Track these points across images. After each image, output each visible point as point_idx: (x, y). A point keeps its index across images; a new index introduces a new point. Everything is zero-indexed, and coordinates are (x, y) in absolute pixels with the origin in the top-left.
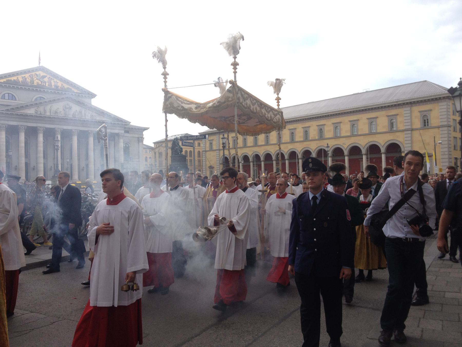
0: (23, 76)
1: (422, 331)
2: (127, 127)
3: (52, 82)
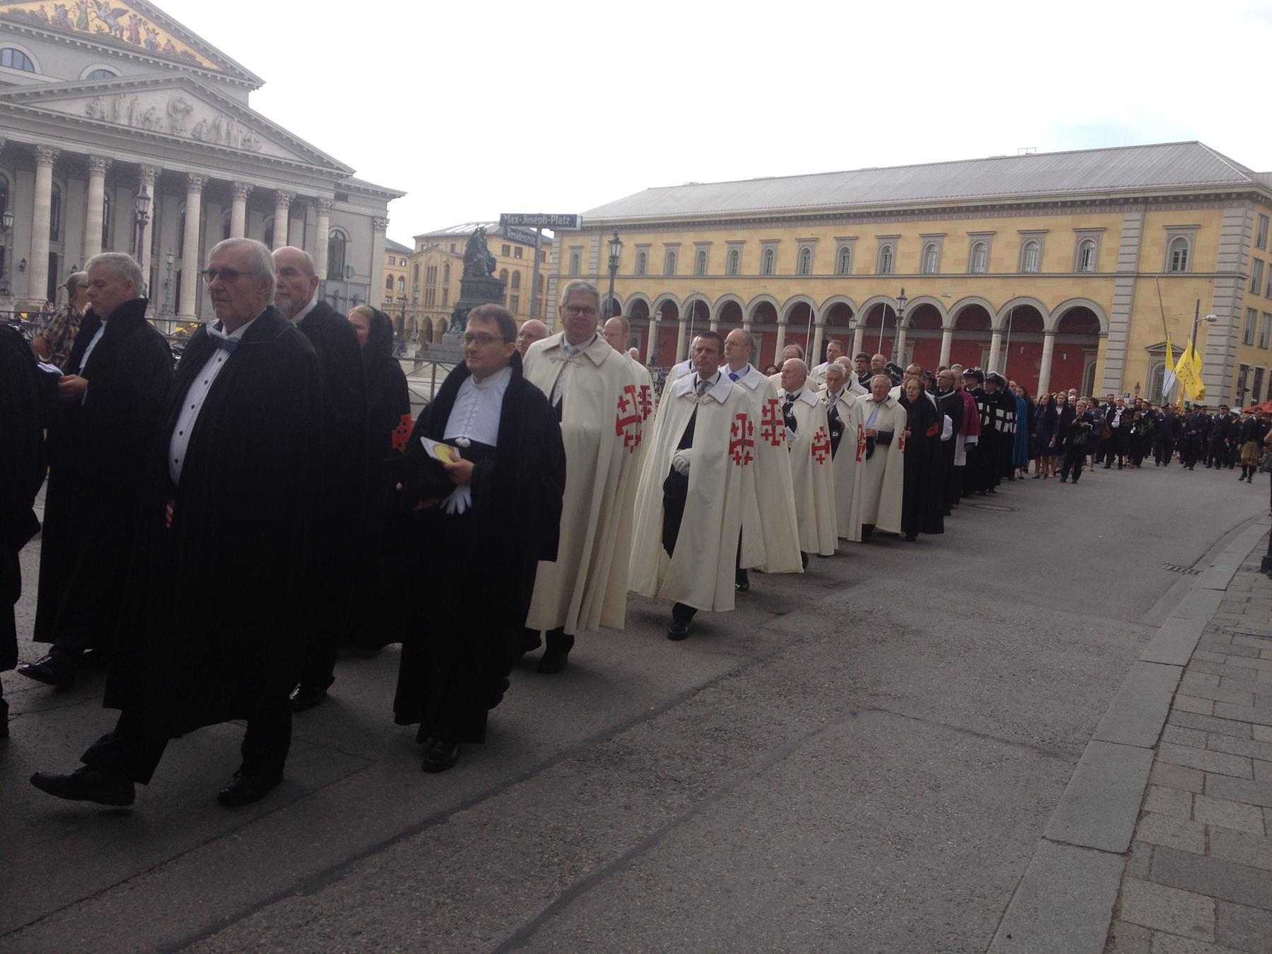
1: (1207, 834)
2: (344, 182)
3: (142, 30)
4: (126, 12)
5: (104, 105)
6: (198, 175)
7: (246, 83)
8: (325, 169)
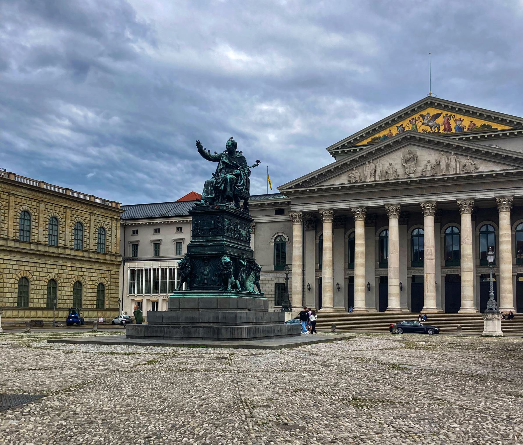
0: (398, 125)
4: (441, 113)
5: (356, 174)
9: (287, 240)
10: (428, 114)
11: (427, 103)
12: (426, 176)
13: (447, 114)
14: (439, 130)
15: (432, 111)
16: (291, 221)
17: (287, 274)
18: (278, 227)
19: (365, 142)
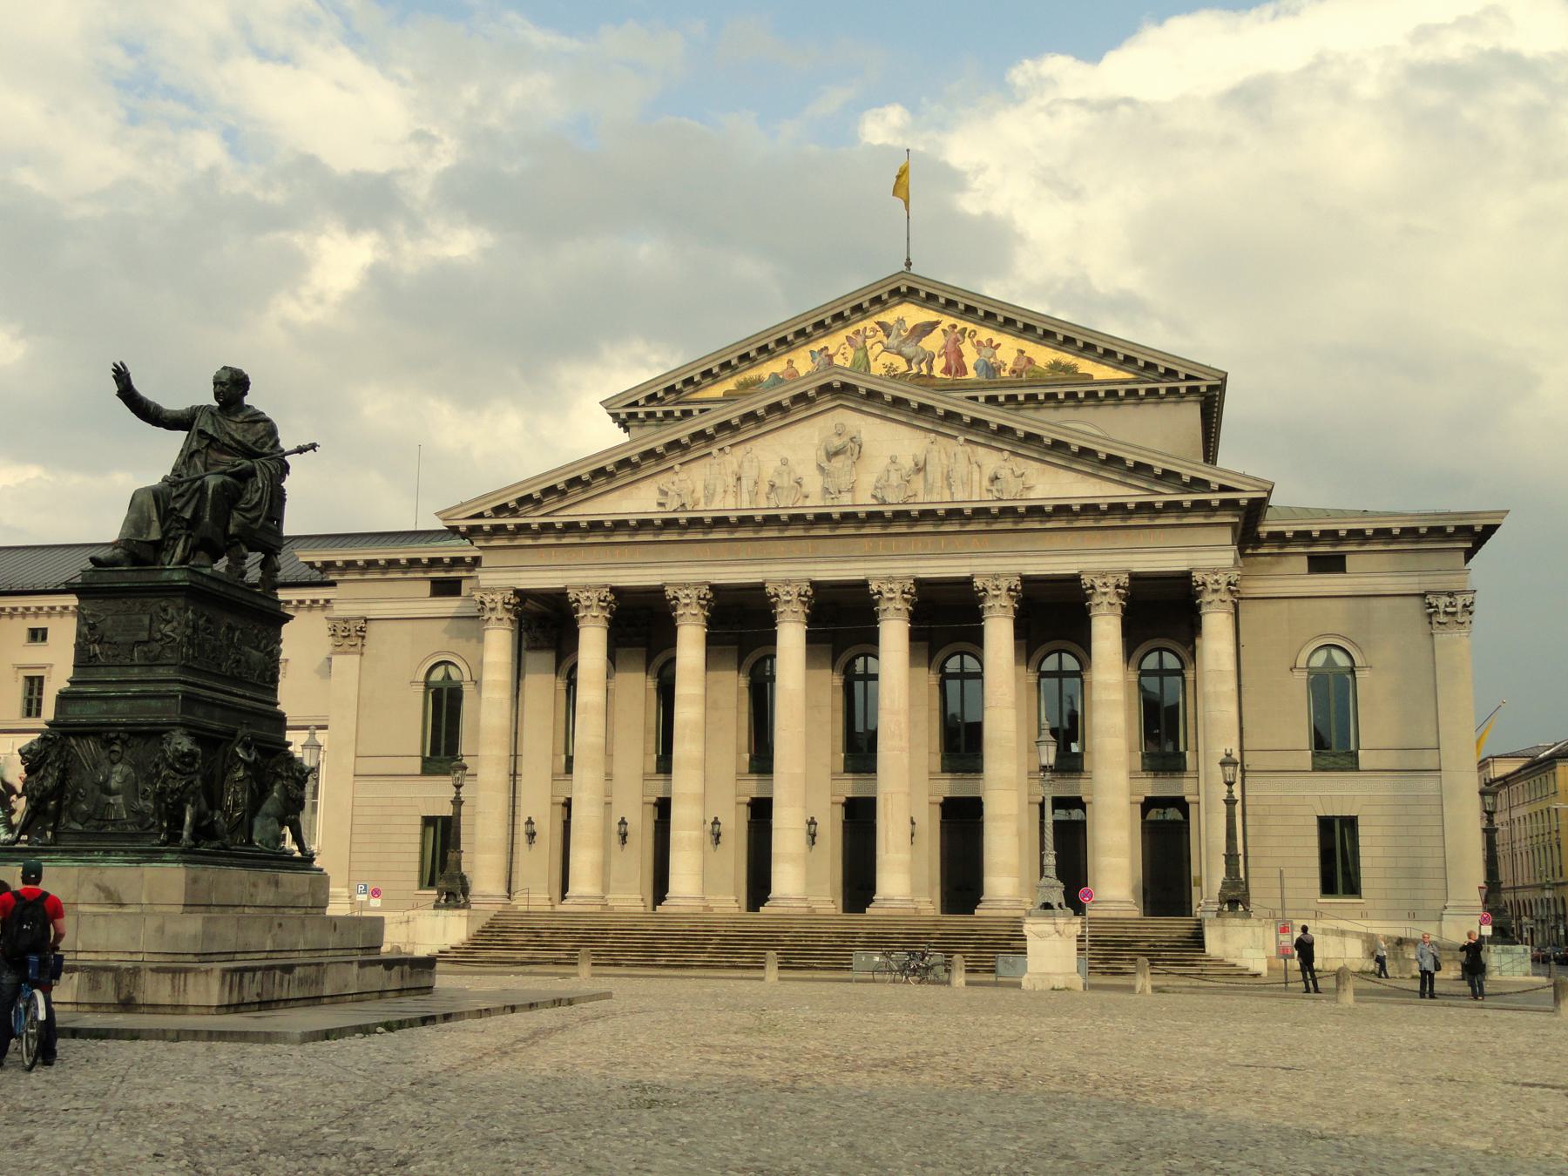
0: (816, 347)
4: (938, 323)
6: (890, 579)
7: (1183, 387)
8: (1187, 499)
9: (467, 677)
10: (901, 321)
11: (898, 289)
12: (884, 503)
13: (954, 326)
14: (930, 368)
15: (912, 314)
16: (474, 621)
17: (458, 787)
18: (437, 642)
19: (716, 391)
